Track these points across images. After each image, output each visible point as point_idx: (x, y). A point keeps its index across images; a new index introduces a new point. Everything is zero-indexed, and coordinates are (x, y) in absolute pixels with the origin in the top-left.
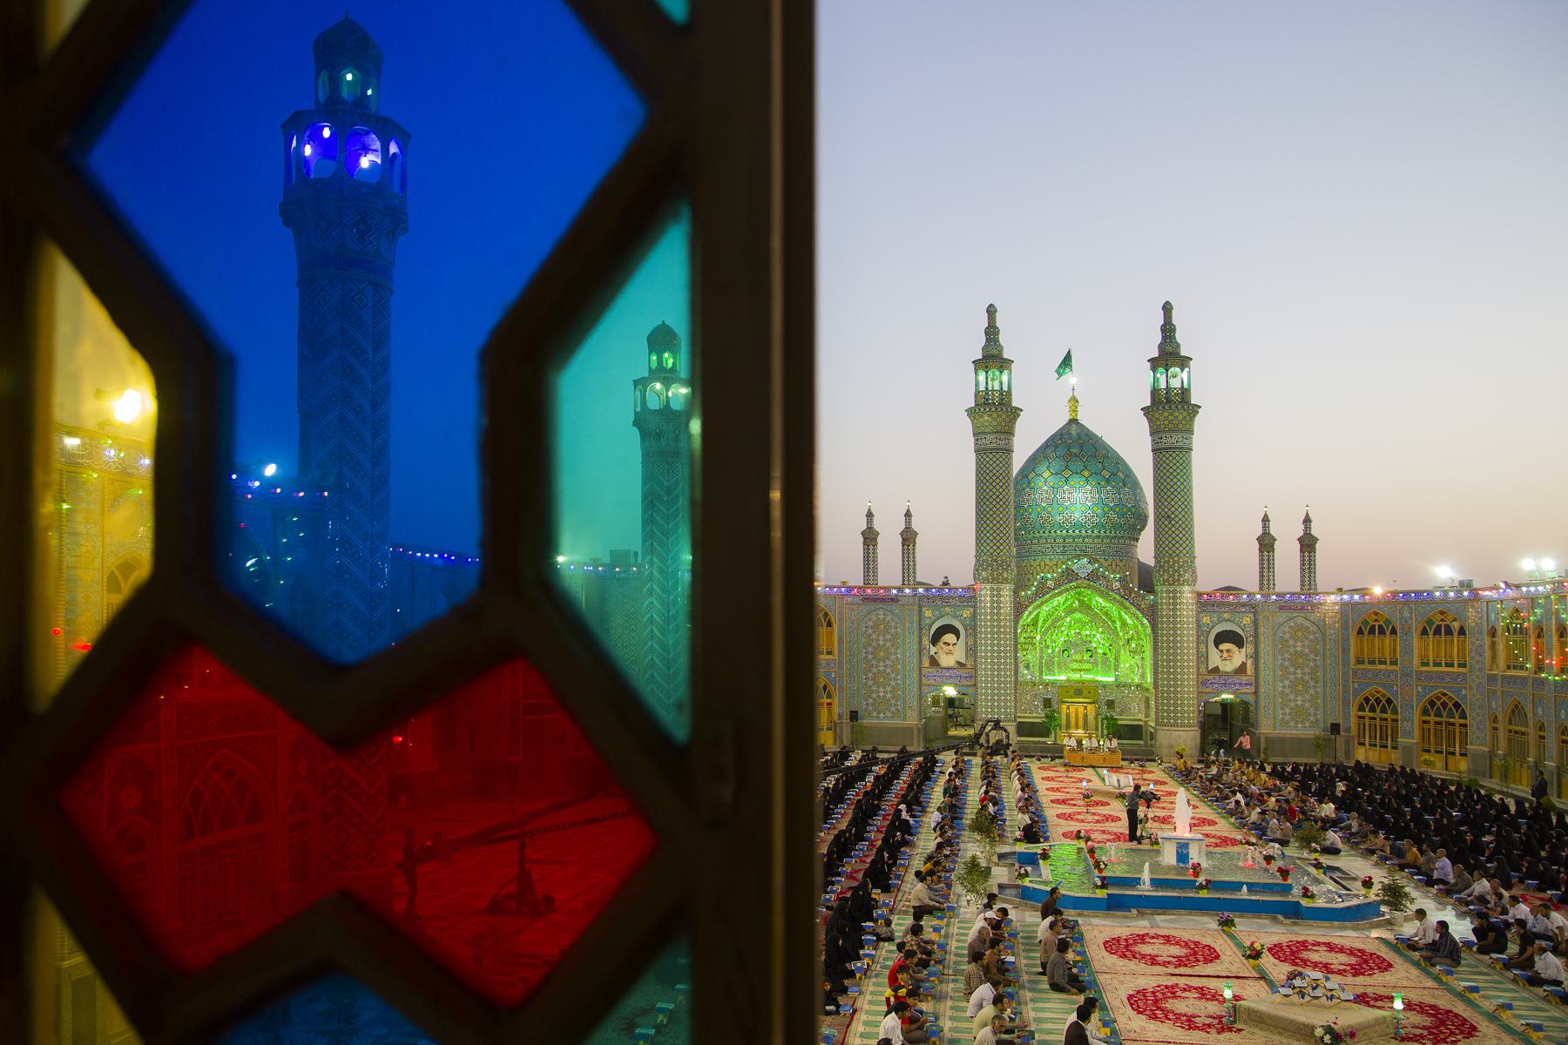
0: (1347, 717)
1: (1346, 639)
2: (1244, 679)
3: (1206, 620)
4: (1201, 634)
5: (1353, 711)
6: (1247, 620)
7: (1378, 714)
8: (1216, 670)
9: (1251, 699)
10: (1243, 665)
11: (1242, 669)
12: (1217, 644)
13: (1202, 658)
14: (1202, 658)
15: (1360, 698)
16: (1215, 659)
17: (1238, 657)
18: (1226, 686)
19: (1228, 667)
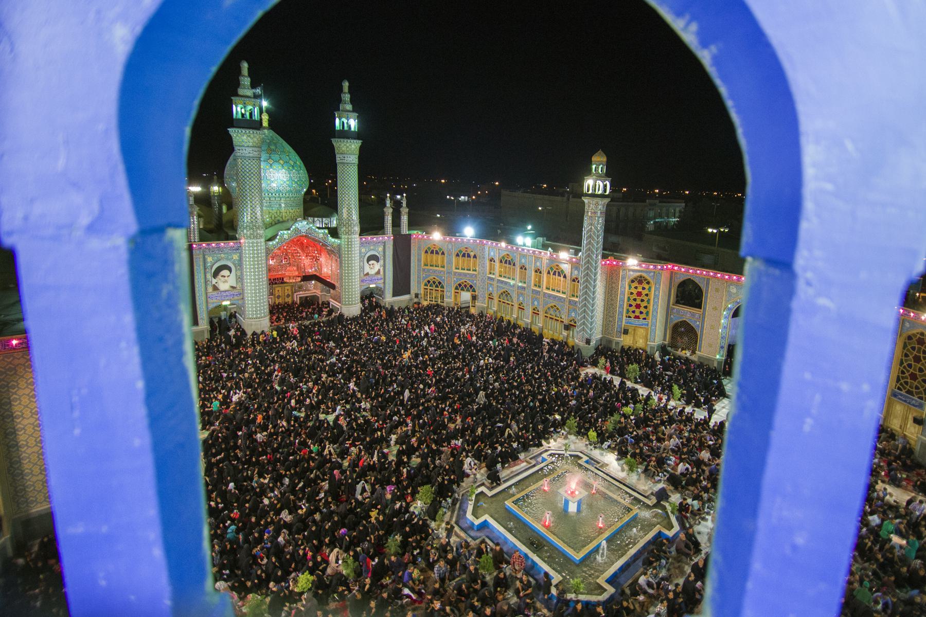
0: (419, 288)
1: (419, 255)
2: (379, 277)
3: (363, 250)
4: (361, 257)
5: (423, 286)
6: (381, 249)
7: (434, 288)
8: (367, 274)
9: (382, 286)
10: (379, 271)
11: (378, 273)
12: (368, 260)
13: (362, 268)
14: (362, 268)
15: (426, 281)
16: (367, 269)
17: (377, 266)
18: (372, 281)
19: (372, 272)
